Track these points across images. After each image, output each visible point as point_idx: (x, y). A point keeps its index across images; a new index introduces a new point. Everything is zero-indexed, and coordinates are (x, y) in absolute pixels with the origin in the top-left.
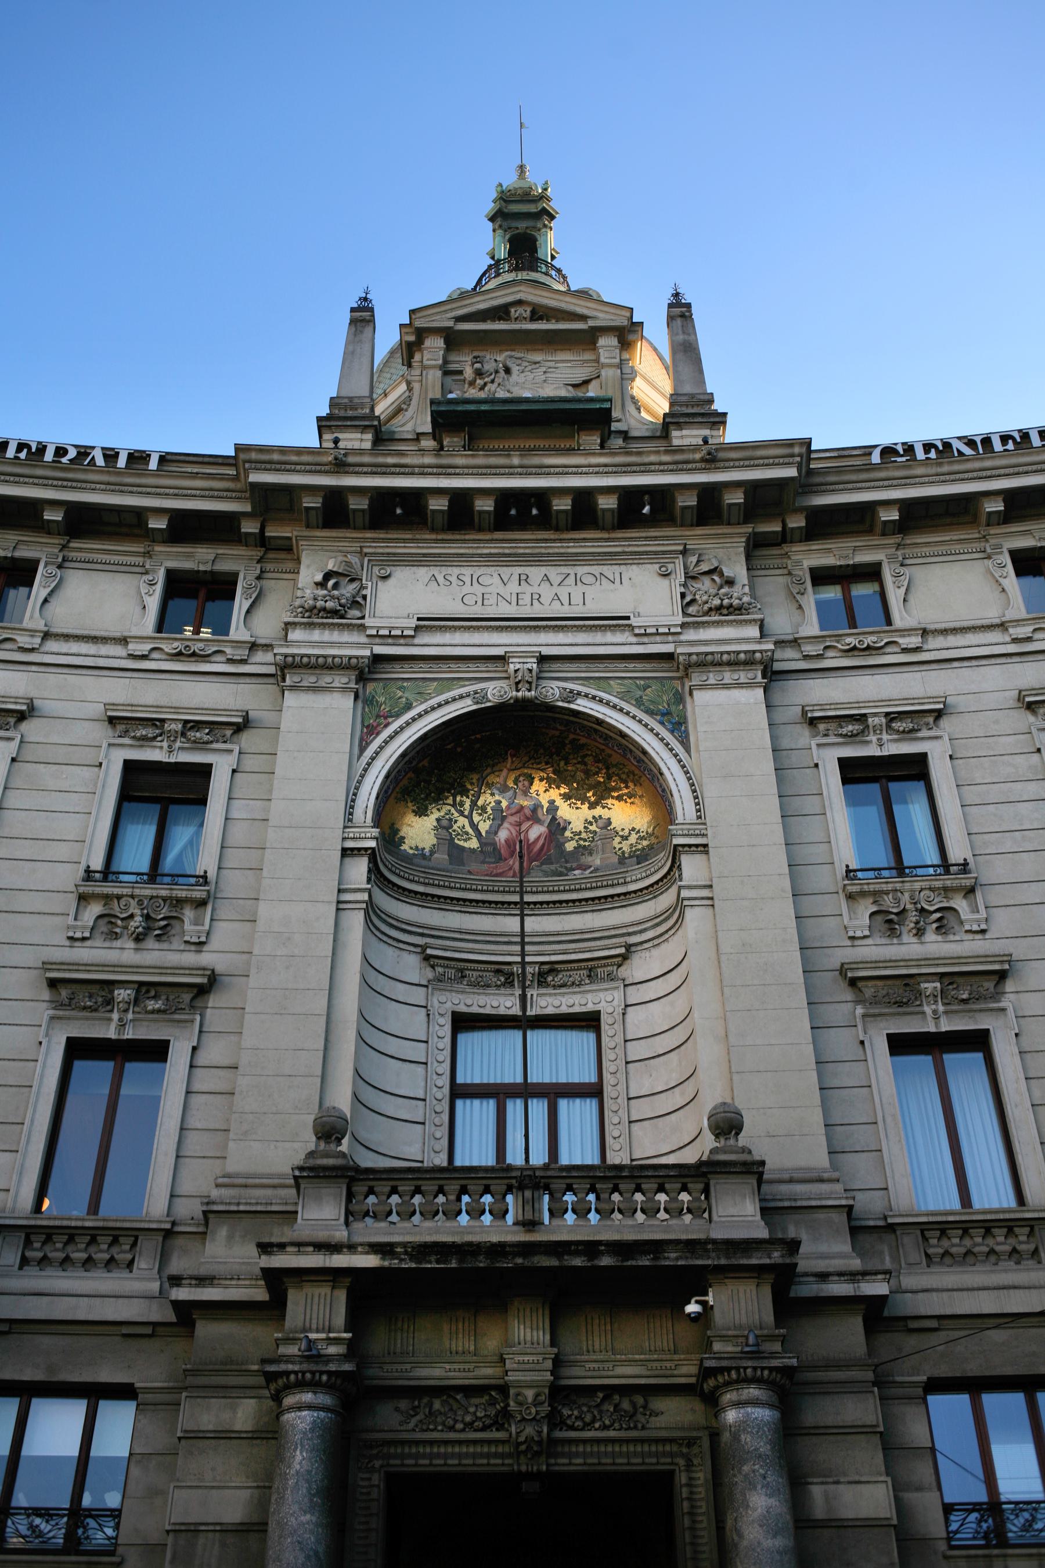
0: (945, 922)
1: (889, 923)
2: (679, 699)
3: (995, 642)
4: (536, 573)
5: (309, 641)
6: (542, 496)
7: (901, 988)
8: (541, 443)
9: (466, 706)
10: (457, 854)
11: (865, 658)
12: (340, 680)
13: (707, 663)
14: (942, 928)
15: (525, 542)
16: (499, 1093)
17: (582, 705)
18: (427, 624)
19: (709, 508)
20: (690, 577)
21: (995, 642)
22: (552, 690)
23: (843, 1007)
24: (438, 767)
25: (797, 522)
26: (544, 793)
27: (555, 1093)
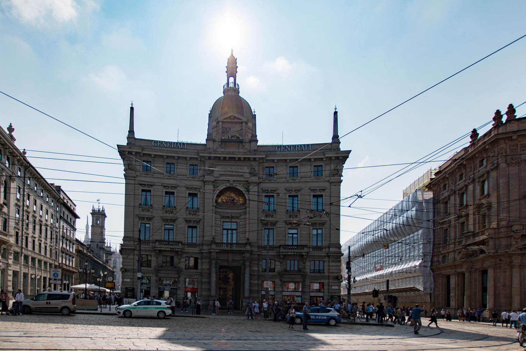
0: (272, 216)
1: (267, 216)
2: (248, 186)
3: (284, 180)
4: (233, 167)
5: (207, 178)
6: (234, 158)
7: (266, 224)
8: (234, 164)
9: (225, 187)
10: (223, 202)
11: (270, 182)
12: (211, 183)
13: (251, 183)
14: (272, 217)
15: (232, 163)
16: (228, 230)
17: (237, 187)
18: (221, 175)
19: (255, 159)
20: (251, 169)
21: (284, 180)
22: (234, 185)
23: (260, 225)
24: (221, 193)
25: (265, 161)
26: (233, 195)
27: (232, 230)
